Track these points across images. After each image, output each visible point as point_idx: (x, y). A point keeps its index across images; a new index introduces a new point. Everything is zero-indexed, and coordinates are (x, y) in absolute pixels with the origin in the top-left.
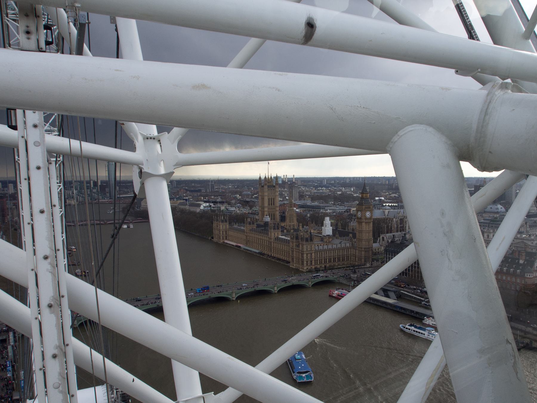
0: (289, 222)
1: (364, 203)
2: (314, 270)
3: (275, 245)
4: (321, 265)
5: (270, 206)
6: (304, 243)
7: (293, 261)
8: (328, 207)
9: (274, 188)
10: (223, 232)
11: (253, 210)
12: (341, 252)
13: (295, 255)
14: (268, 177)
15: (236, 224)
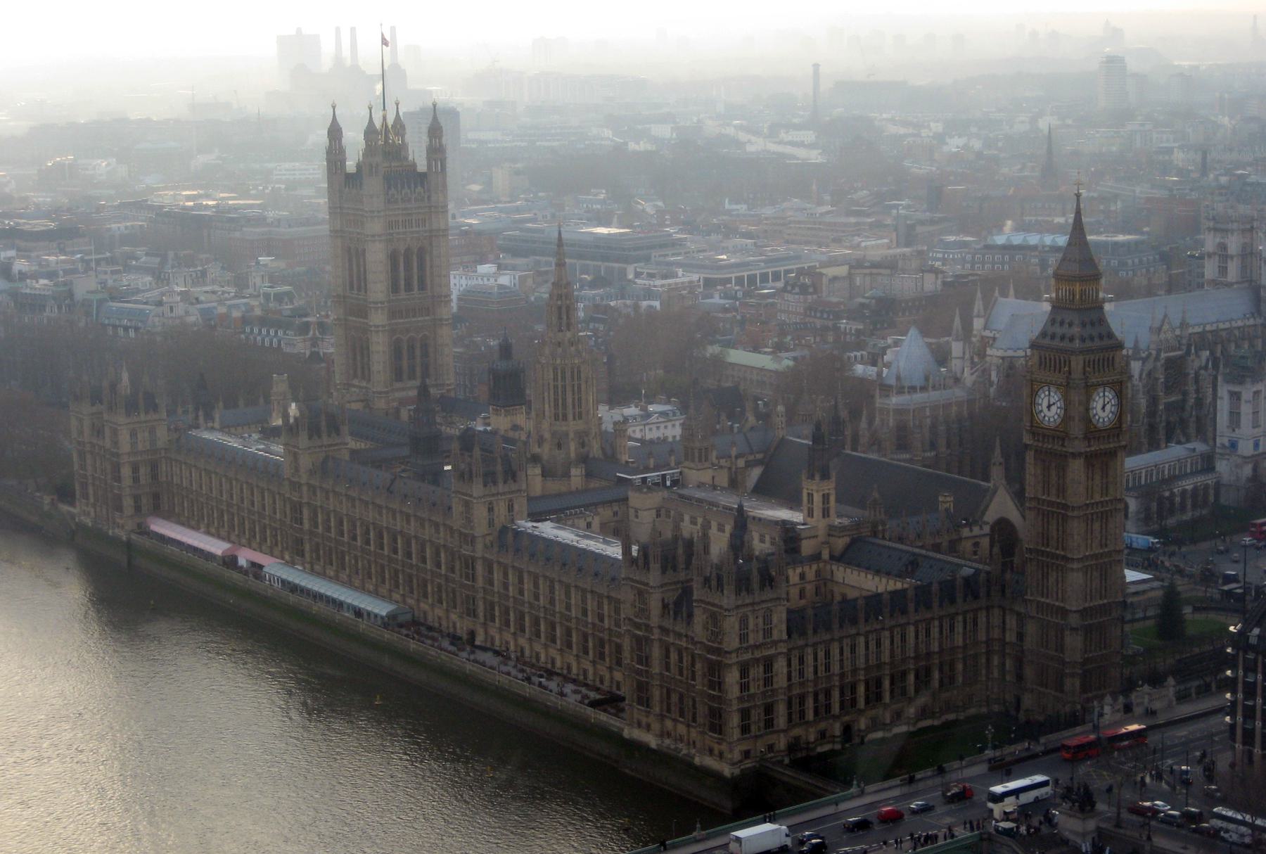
0: (556, 418)
1: (1083, 340)
2: (787, 761)
3: (497, 576)
4: (823, 725)
5: (403, 295)
6: (728, 599)
7: (645, 701)
8: (662, 246)
9: (419, 189)
10: (135, 469)
11: (267, 296)
12: (935, 632)
13: (656, 669)
14: (386, 126)
15: (209, 417)
